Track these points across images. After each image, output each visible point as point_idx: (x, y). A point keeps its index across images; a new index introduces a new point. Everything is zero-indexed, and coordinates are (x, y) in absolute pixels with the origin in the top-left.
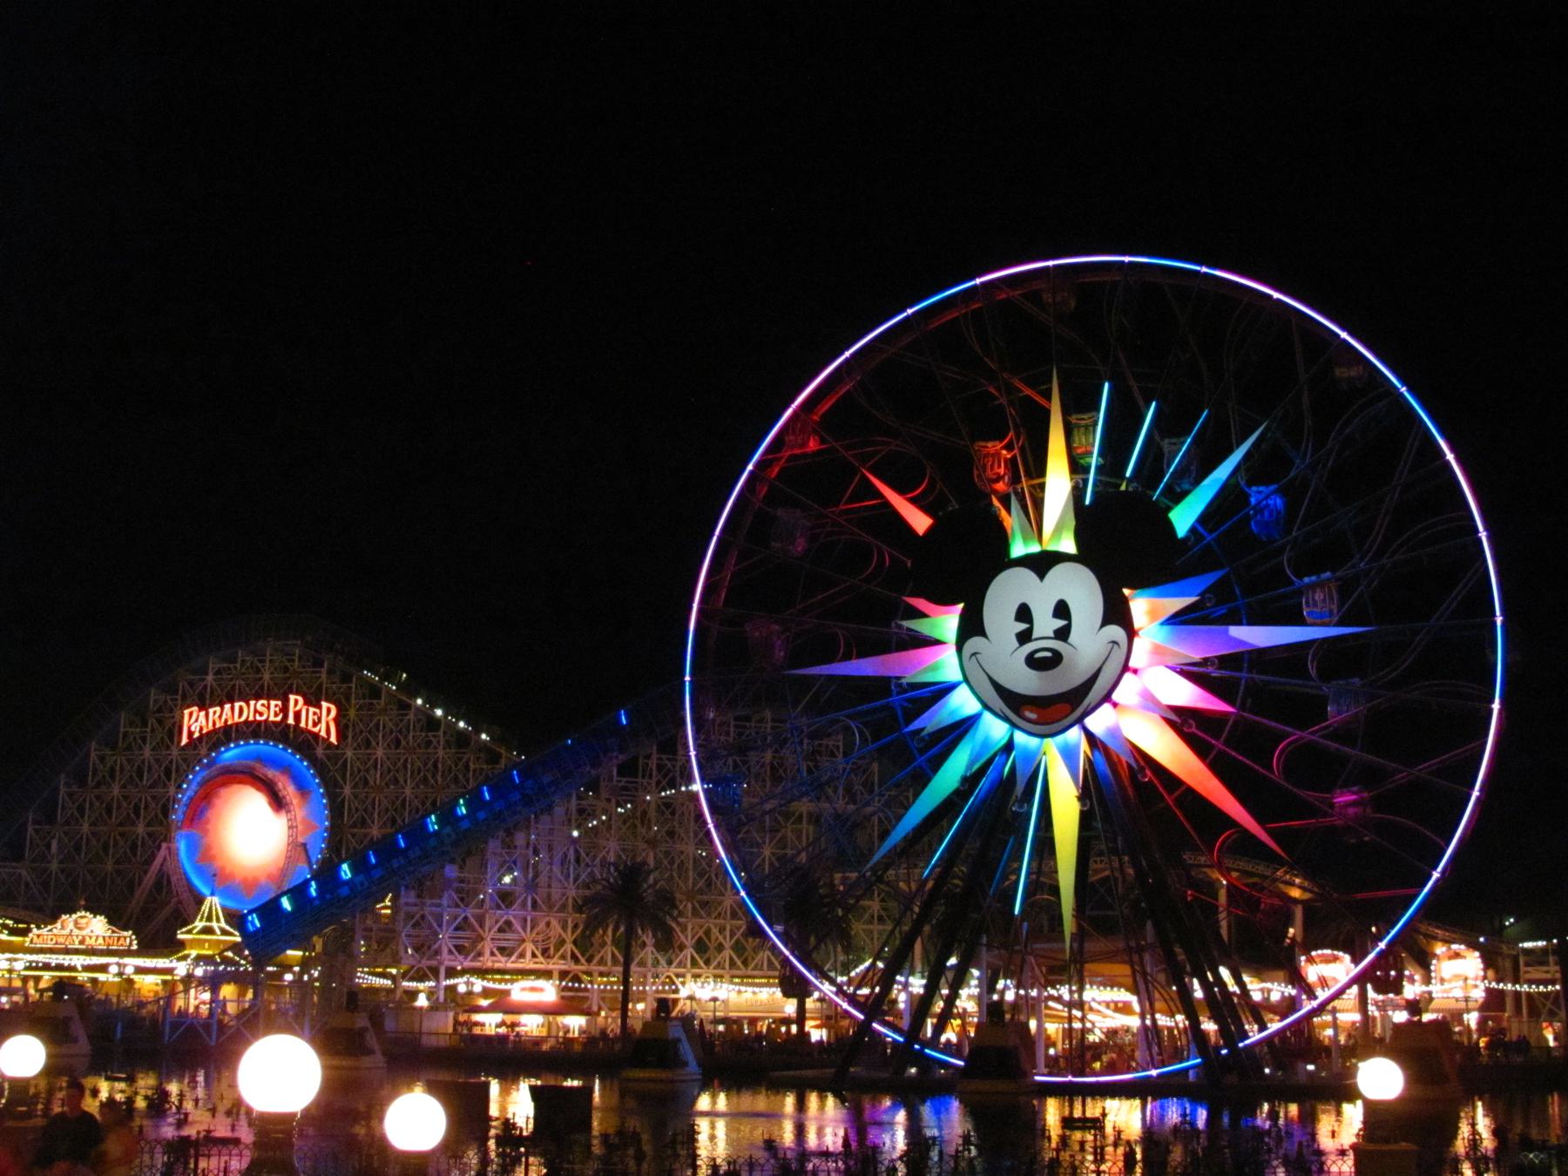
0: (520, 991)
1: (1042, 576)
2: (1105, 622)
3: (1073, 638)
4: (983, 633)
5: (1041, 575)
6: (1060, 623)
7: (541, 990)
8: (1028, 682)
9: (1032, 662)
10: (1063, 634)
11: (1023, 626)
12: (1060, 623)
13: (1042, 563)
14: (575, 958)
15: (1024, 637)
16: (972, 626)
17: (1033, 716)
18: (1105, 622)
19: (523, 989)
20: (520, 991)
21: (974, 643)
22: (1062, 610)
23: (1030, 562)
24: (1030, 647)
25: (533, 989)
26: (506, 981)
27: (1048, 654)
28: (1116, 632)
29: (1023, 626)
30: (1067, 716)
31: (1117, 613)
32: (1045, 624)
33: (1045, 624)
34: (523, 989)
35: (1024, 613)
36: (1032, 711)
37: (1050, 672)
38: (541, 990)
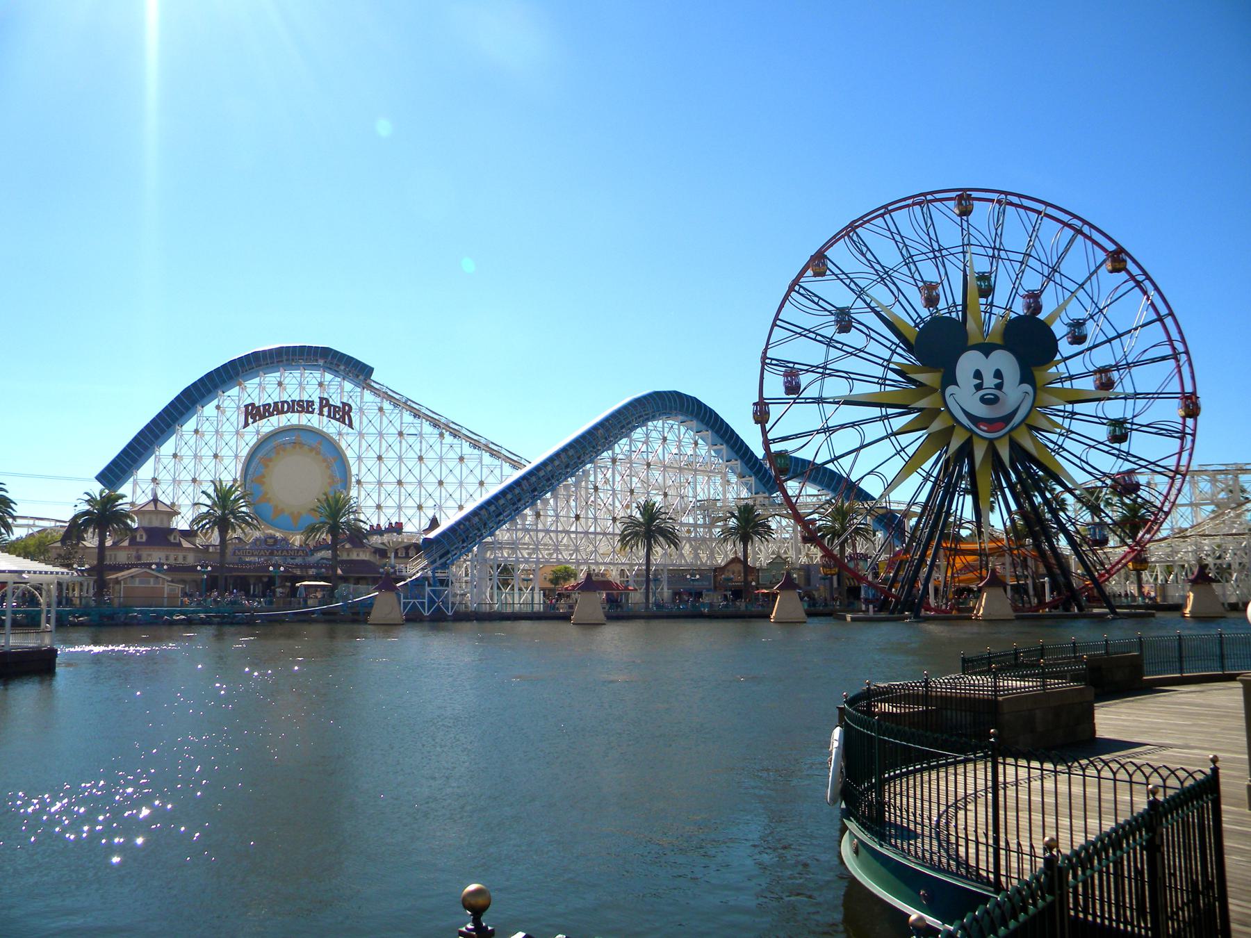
1: (987, 355)
2: (1022, 382)
3: (1005, 389)
5: (987, 355)
8: (981, 410)
9: (983, 400)
10: (999, 387)
13: (986, 349)
15: (979, 387)
16: (950, 379)
17: (985, 428)
18: (1022, 382)
21: (951, 389)
22: (998, 374)
28: (1027, 387)
30: (1004, 428)
31: (1027, 377)
32: (990, 381)
33: (990, 381)
35: (978, 375)
36: (985, 426)
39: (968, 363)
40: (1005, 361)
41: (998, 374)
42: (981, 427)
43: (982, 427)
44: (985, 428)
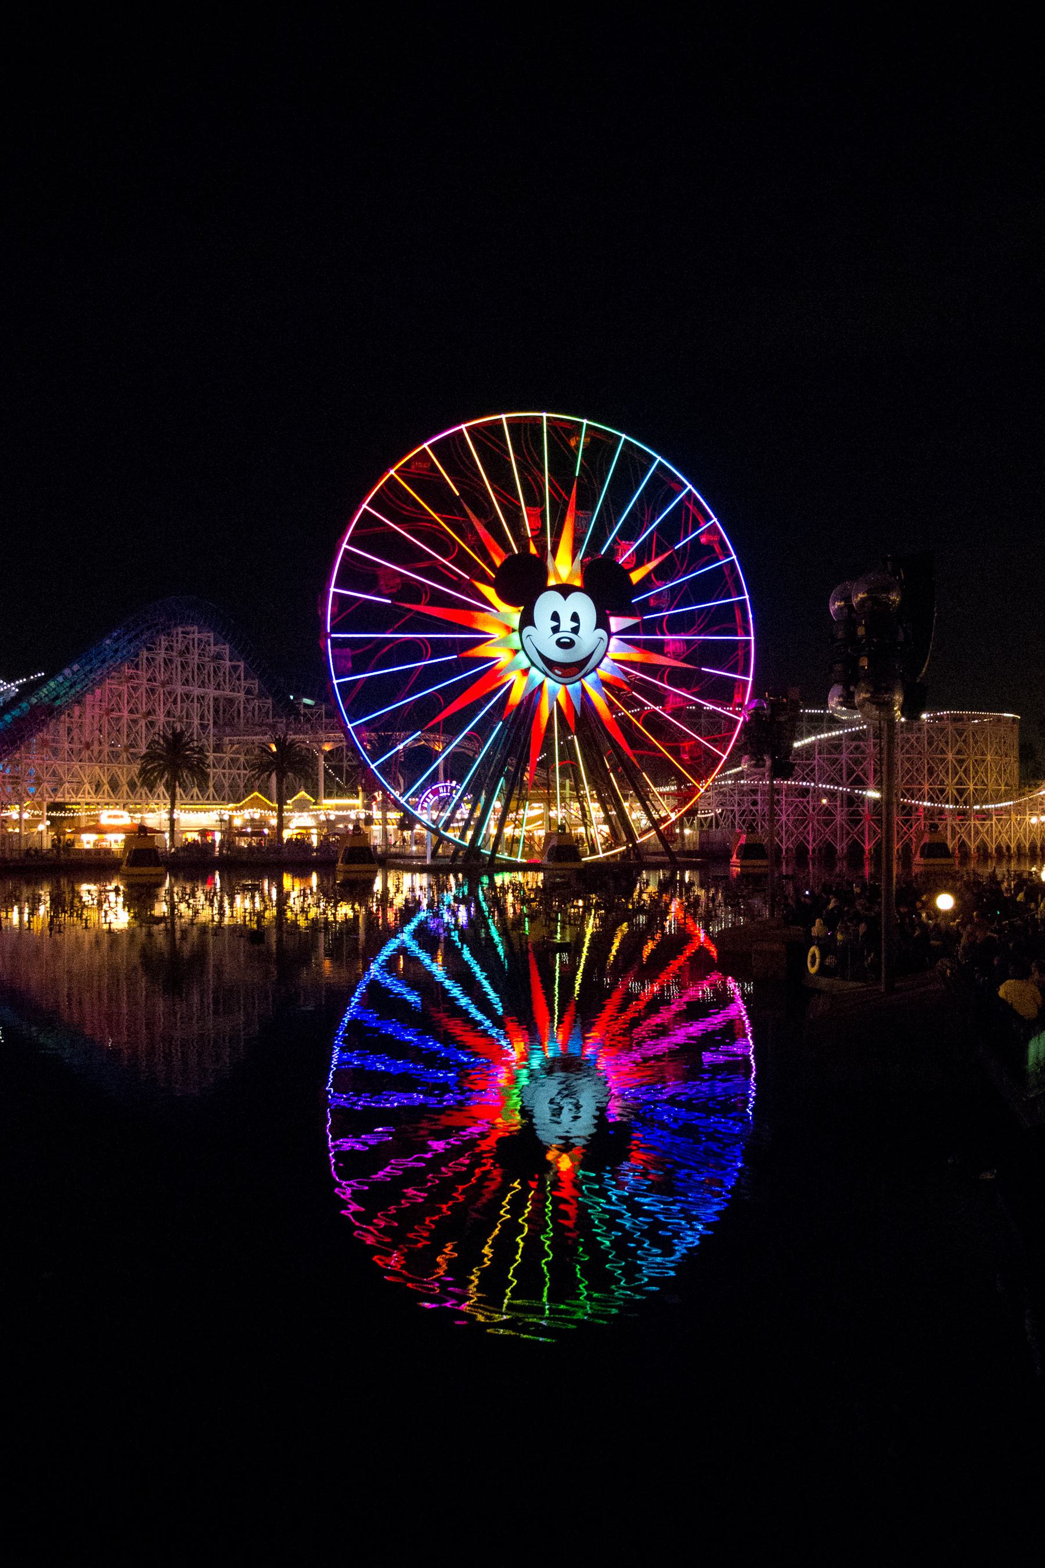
0: (106, 817)
1: (565, 596)
2: (596, 628)
4: (534, 626)
5: (565, 596)
6: (575, 624)
7: (122, 817)
8: (558, 655)
9: (560, 644)
10: (575, 630)
11: (555, 624)
12: (575, 624)
13: (565, 590)
14: (109, 796)
15: (555, 630)
16: (527, 620)
17: (560, 673)
18: (596, 628)
19: (110, 817)
20: (106, 817)
21: (528, 630)
22: (575, 617)
23: (555, 588)
24: (558, 635)
25: (116, 817)
26: (94, 809)
27: (568, 641)
28: (602, 633)
29: (555, 624)
31: (602, 623)
32: (566, 624)
33: (566, 624)
34: (110, 817)
35: (555, 617)
37: (570, 650)
38: (122, 817)
39: (547, 604)
40: (583, 605)
41: (575, 617)
42: (556, 671)
43: (556, 671)
44: (560, 673)
